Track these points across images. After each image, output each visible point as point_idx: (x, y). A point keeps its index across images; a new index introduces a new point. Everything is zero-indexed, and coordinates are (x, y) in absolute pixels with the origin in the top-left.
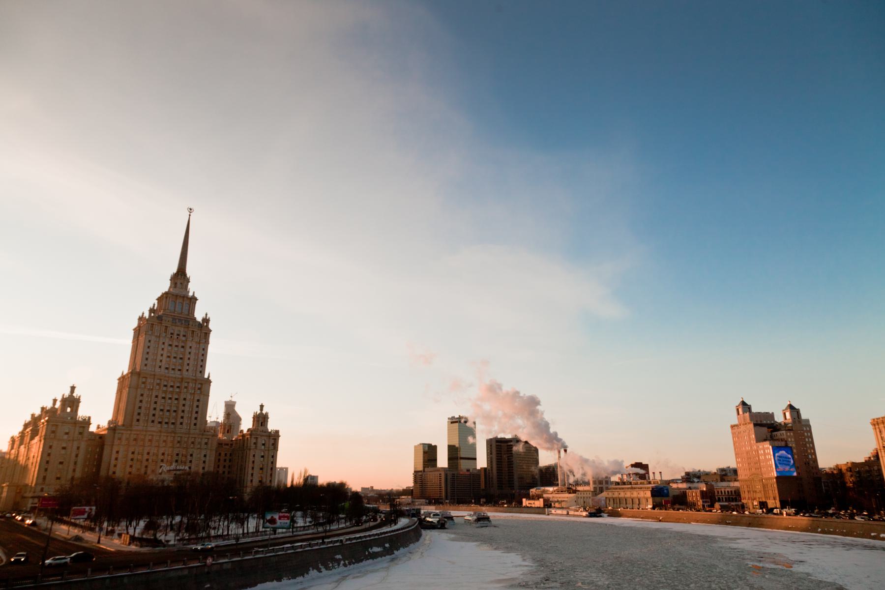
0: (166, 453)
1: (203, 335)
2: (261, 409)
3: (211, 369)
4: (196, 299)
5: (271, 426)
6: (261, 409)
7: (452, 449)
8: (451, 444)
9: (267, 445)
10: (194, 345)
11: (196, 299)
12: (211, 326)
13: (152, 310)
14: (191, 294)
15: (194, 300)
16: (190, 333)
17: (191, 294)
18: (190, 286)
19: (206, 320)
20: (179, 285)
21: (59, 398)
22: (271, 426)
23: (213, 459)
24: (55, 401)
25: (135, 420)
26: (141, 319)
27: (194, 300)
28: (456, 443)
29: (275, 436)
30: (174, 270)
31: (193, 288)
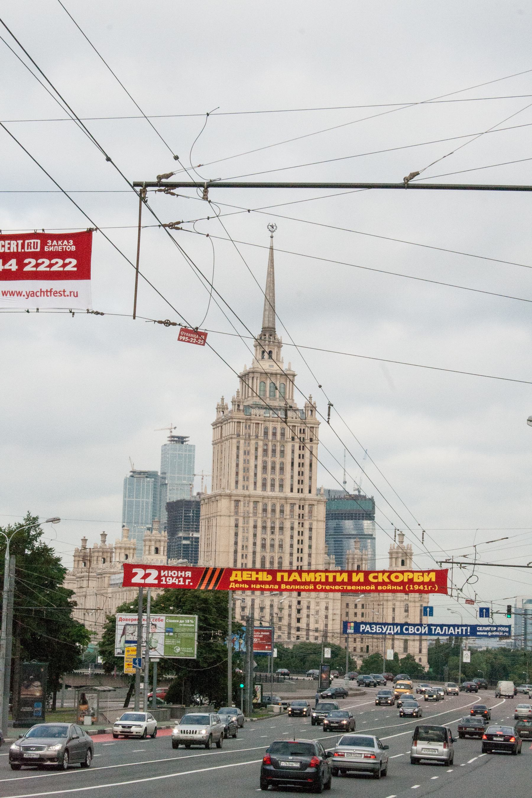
4: (294, 375)
11: (294, 375)
23: (338, 612)
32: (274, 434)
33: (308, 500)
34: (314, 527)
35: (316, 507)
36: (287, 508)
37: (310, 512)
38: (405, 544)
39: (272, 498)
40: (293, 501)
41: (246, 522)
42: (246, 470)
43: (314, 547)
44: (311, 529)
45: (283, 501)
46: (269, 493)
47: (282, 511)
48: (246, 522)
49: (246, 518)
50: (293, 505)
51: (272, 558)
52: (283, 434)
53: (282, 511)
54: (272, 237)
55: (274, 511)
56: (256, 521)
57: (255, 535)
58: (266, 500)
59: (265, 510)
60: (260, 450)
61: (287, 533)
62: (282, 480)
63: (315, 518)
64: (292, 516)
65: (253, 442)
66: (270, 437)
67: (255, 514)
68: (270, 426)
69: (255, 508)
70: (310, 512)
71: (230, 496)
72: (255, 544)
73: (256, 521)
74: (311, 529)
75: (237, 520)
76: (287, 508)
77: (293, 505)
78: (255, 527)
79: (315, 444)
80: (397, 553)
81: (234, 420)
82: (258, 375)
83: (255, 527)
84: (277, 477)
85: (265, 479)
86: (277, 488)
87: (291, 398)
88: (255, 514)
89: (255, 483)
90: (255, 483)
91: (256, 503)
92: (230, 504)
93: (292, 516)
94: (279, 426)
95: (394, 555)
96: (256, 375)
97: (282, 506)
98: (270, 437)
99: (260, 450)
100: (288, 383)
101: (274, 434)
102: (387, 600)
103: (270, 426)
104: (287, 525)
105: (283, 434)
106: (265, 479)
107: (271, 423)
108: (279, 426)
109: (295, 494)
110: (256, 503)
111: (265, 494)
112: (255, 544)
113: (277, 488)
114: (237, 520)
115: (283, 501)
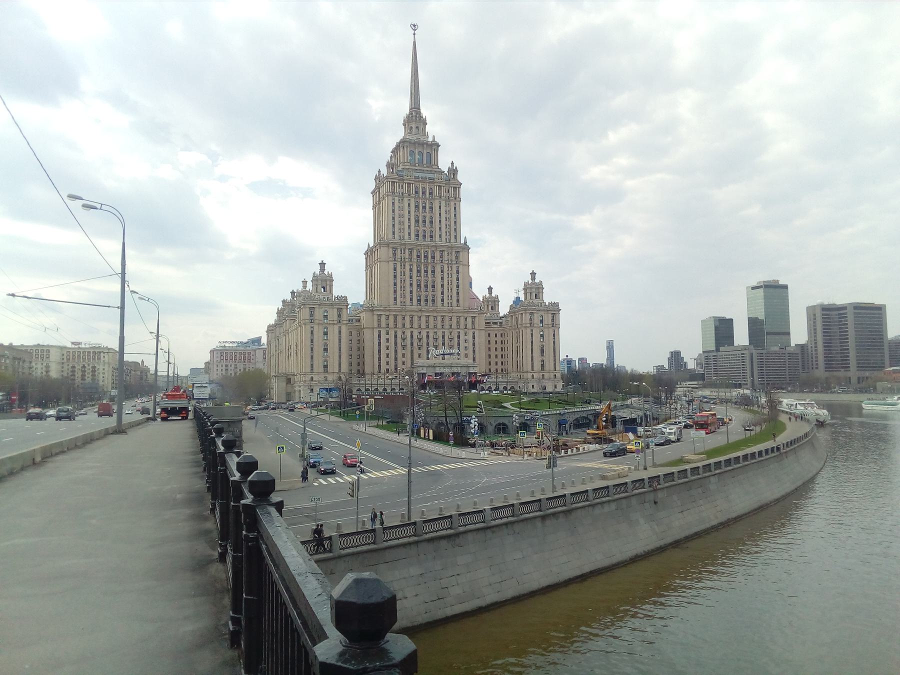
1: (452, 190)
2: (533, 278)
3: (466, 232)
4: (438, 146)
5: (548, 298)
6: (533, 278)
7: (754, 325)
8: (751, 316)
11: (438, 146)
12: (460, 177)
13: (390, 165)
14: (430, 139)
15: (435, 146)
17: (430, 139)
18: (428, 128)
19: (453, 171)
20: (414, 129)
21: (309, 279)
22: (547, 298)
24: (305, 282)
26: (378, 178)
27: (435, 146)
28: (761, 316)
29: (554, 310)
30: (406, 110)
31: (433, 130)
32: (424, 193)
34: (460, 270)
36: (437, 255)
37: (457, 257)
40: (442, 249)
41: (403, 266)
42: (401, 223)
44: (458, 272)
45: (433, 249)
46: (421, 242)
47: (433, 257)
48: (403, 266)
49: (403, 263)
50: (442, 252)
51: (426, 296)
52: (431, 193)
53: (433, 257)
55: (426, 257)
56: (411, 265)
57: (411, 292)
59: (419, 257)
60: (413, 206)
62: (434, 296)
64: (442, 261)
65: (406, 200)
66: (421, 195)
67: (410, 260)
68: (421, 186)
69: (410, 255)
70: (457, 257)
71: (388, 245)
72: (411, 285)
73: (411, 265)
74: (458, 272)
75: (395, 265)
76: (437, 255)
77: (442, 252)
78: (411, 270)
80: (531, 288)
83: (411, 270)
84: (428, 230)
85: (417, 231)
86: (430, 302)
88: (410, 260)
89: (409, 234)
90: (409, 234)
91: (411, 250)
93: (442, 261)
96: (406, 144)
97: (433, 252)
98: (421, 195)
99: (413, 206)
101: (424, 193)
103: (421, 186)
104: (438, 269)
105: (431, 193)
106: (417, 231)
108: (427, 187)
109: (443, 243)
110: (411, 250)
111: (418, 243)
112: (411, 285)
113: (430, 302)
114: (395, 265)
115: (433, 249)
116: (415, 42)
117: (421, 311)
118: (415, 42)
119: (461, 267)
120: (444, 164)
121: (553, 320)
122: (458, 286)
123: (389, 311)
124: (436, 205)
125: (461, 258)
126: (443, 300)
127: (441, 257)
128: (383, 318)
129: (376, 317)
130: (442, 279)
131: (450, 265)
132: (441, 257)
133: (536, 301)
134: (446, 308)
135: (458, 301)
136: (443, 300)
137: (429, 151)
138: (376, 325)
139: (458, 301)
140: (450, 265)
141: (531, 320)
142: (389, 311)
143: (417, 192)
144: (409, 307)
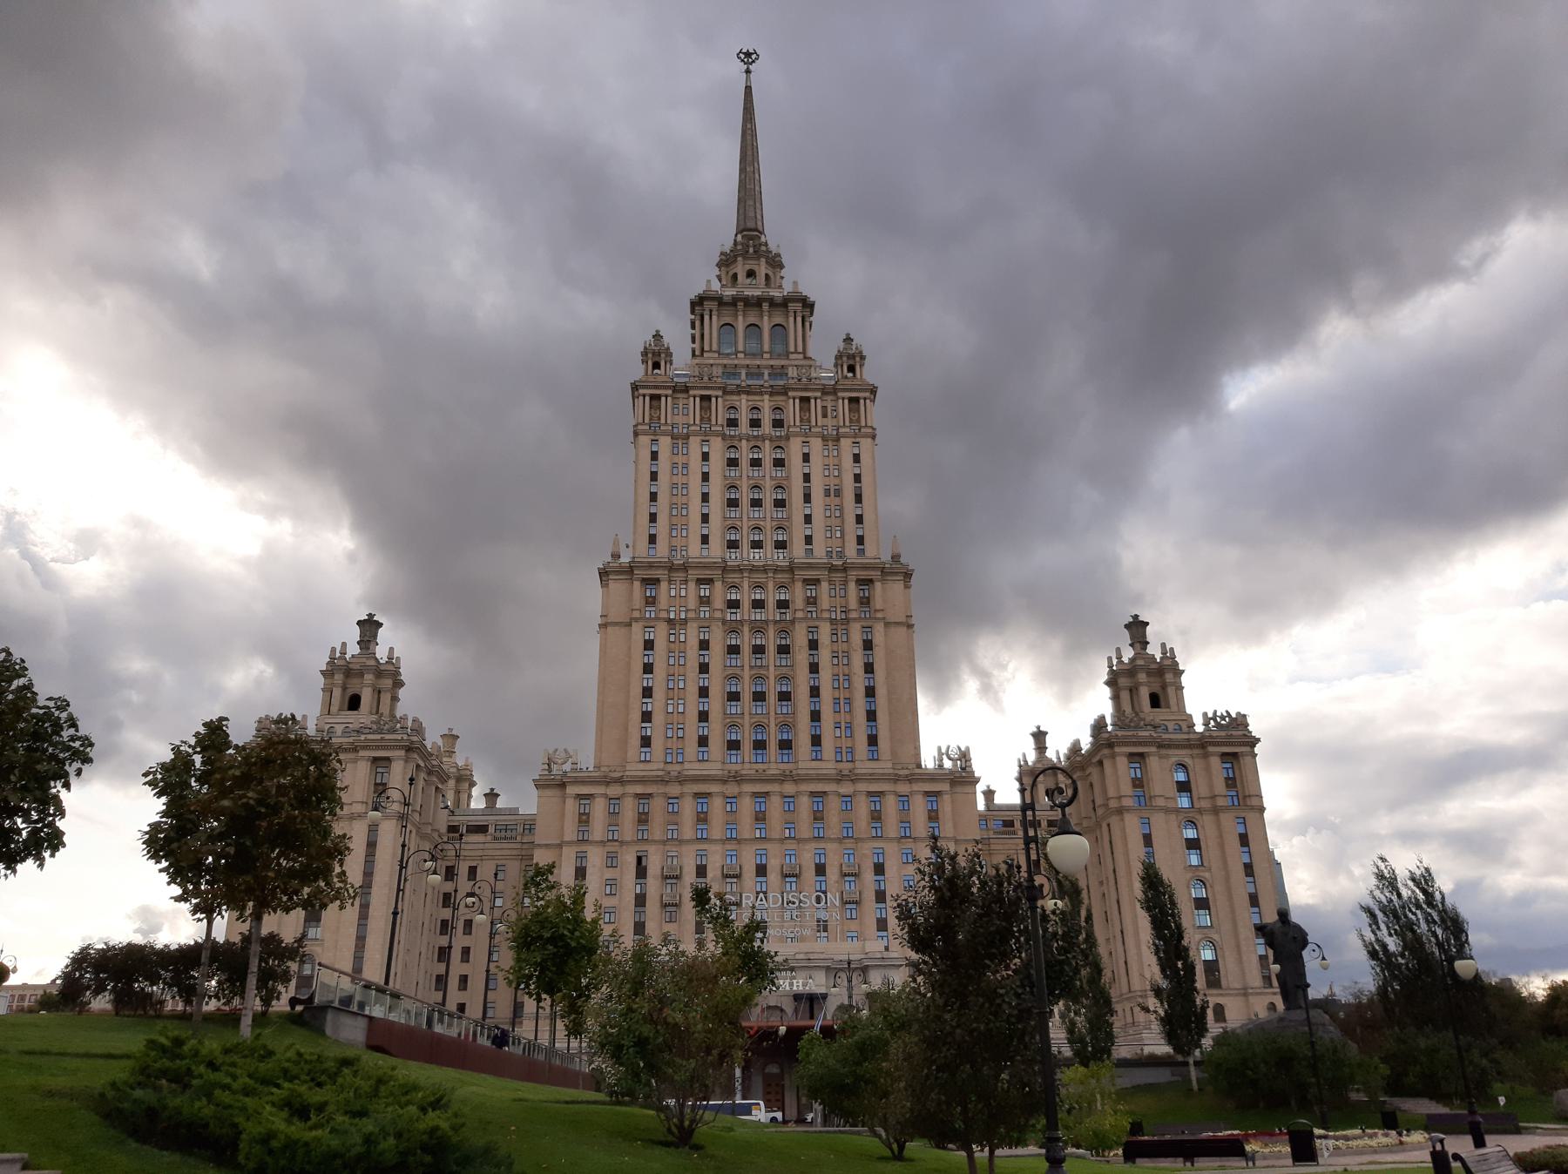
0: (774, 865)
1: (843, 407)
4: (808, 305)
9: (1200, 787)
10: (816, 445)
16: (792, 411)
19: (850, 360)
25: (635, 741)
33: (855, 567)
34: (879, 637)
35: (878, 585)
37: (865, 602)
38: (1154, 650)
39: (753, 569)
43: (881, 692)
44: (868, 645)
54: (748, 71)
58: (733, 578)
61: (802, 656)
63: (879, 615)
70: (865, 602)
71: (629, 570)
74: (868, 645)
76: (798, 594)
79: (866, 436)
81: (642, 391)
82: (713, 305)
87: (800, 349)
92: (631, 592)
94: (766, 403)
95: (1123, 681)
100: (791, 319)
102: (1120, 811)
103: (743, 402)
104: (800, 638)
107: (744, 397)
108: (766, 403)
116: (748, 89)
117: (738, 778)
118: (748, 89)
119: (879, 628)
120: (823, 351)
121: (1231, 782)
122: (870, 692)
123: (620, 781)
124: (795, 448)
125: (878, 603)
126: (816, 741)
127: (812, 601)
128: (599, 809)
129: (571, 807)
130: (814, 668)
131: (841, 624)
132: (812, 601)
133: (1159, 715)
134: (828, 767)
135: (873, 740)
136: (816, 741)
137: (778, 320)
138: (570, 833)
139: (873, 740)
140: (841, 624)
141: (1138, 783)
142: (620, 781)
143: (733, 423)
144: (693, 769)
